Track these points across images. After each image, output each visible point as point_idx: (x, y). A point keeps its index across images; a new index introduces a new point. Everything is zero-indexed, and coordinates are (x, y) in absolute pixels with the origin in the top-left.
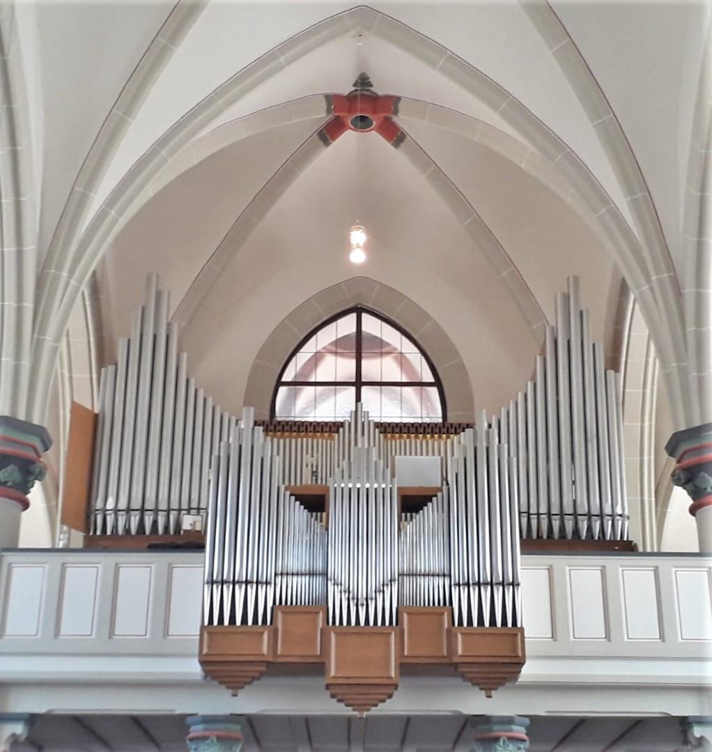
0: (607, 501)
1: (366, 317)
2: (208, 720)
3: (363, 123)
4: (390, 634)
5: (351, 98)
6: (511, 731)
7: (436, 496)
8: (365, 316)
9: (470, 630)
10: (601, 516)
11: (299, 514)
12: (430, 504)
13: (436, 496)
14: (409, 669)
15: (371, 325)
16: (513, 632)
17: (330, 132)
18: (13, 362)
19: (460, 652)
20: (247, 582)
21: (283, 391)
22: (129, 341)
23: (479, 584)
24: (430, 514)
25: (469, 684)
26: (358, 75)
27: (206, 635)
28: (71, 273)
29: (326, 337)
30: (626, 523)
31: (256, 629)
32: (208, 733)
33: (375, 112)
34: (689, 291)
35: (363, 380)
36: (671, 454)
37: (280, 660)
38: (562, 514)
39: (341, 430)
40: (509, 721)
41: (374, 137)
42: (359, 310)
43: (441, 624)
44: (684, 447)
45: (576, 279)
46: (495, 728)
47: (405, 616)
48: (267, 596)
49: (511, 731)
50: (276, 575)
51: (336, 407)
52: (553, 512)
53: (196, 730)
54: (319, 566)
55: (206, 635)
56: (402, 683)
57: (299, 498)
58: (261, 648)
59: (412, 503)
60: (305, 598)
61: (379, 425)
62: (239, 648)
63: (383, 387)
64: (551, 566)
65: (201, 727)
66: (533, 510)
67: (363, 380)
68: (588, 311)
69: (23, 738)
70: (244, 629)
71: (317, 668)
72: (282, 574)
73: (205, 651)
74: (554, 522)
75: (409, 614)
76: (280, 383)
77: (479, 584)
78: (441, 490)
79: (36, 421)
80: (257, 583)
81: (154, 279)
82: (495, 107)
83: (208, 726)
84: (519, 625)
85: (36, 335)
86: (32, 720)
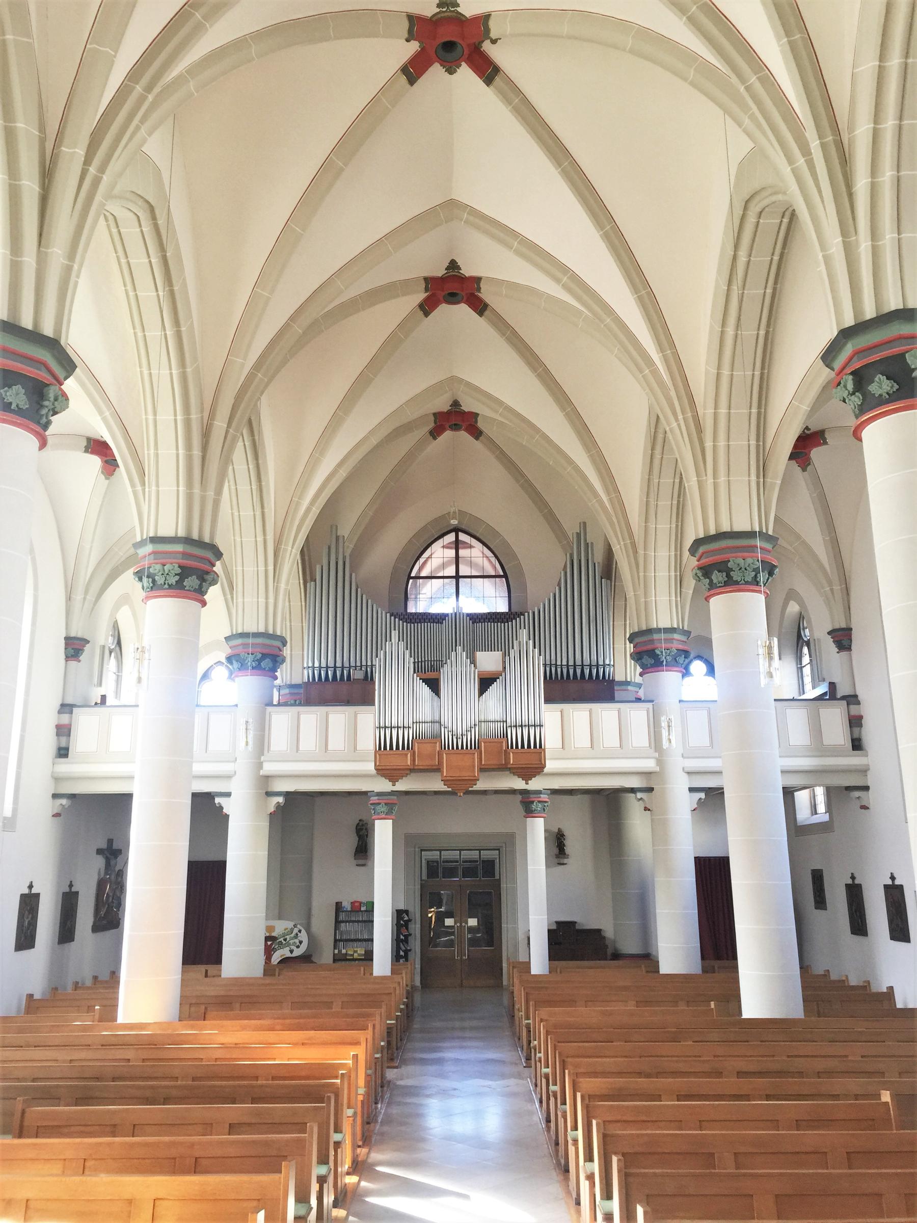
0: (601, 656)
1: (460, 534)
2: (380, 794)
3: (456, 427)
4: (475, 753)
5: (449, 413)
6: (540, 797)
7: (499, 678)
8: (460, 534)
9: (517, 751)
10: (597, 666)
11: (426, 690)
12: (495, 683)
13: (499, 678)
14: (482, 770)
15: (463, 537)
16: (538, 749)
17: (435, 433)
18: (265, 601)
19: (511, 762)
20: (398, 727)
21: (411, 581)
22: (322, 566)
23: (522, 726)
24: (495, 690)
25: (517, 777)
26: (452, 400)
27: (378, 755)
28: (292, 548)
29: (437, 548)
30: (612, 669)
31: (404, 752)
32: (380, 801)
33: (463, 421)
34: (641, 552)
35: (460, 575)
36: (630, 642)
37: (416, 768)
38: (575, 666)
39: (447, 618)
40: (539, 792)
41: (463, 435)
42: (457, 530)
43: (502, 746)
44: (637, 640)
45: (585, 523)
46: (531, 796)
47: (483, 743)
48: (409, 734)
49: (540, 797)
50: (413, 723)
51: (445, 606)
52: (570, 664)
53: (374, 799)
54: (437, 719)
55: (378, 755)
56: (482, 775)
57: (424, 681)
58: (407, 762)
59: (485, 683)
60: (429, 735)
61: (468, 615)
62: (396, 762)
63: (472, 579)
64: (562, 709)
65: (376, 798)
66: (559, 663)
67: (460, 575)
68: (592, 543)
69: (282, 805)
70: (398, 752)
71: (437, 769)
72: (416, 722)
73: (378, 764)
74: (570, 670)
75: (484, 743)
76: (410, 577)
77: (522, 726)
78: (502, 672)
79: (279, 633)
80: (404, 727)
81: (334, 527)
82: (558, 280)
83: (380, 798)
84: (543, 747)
85: (275, 584)
86: (288, 795)
